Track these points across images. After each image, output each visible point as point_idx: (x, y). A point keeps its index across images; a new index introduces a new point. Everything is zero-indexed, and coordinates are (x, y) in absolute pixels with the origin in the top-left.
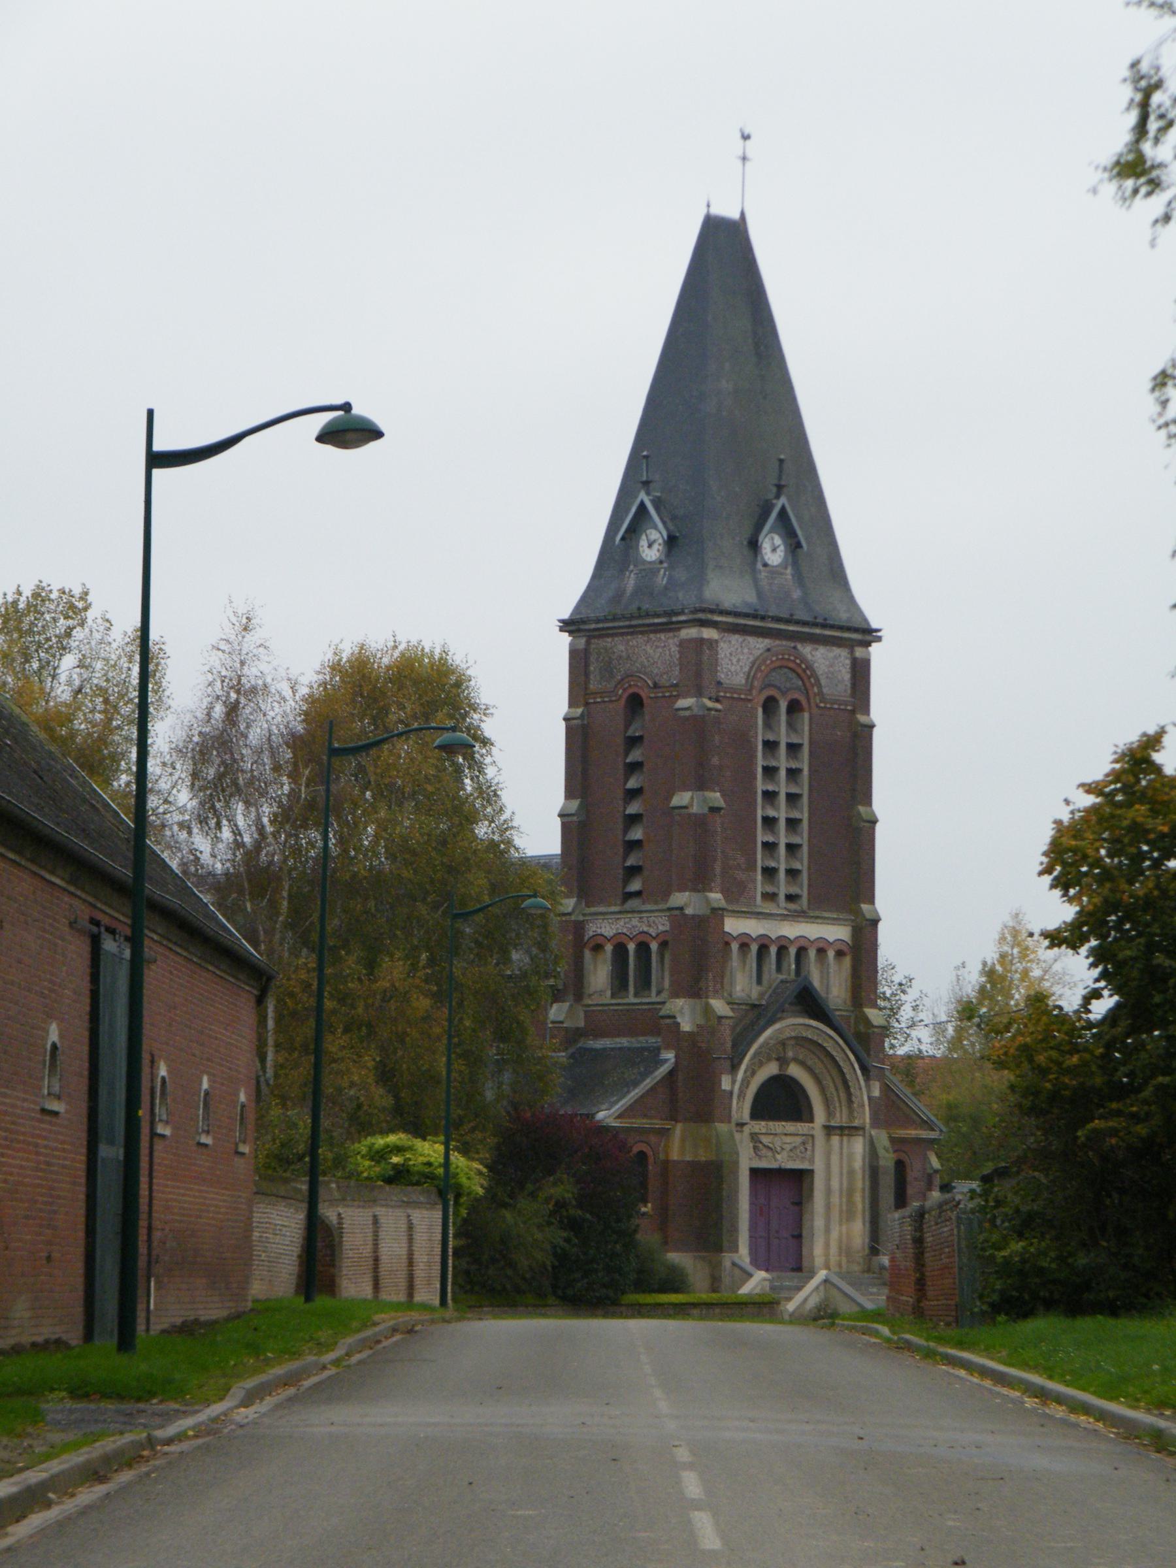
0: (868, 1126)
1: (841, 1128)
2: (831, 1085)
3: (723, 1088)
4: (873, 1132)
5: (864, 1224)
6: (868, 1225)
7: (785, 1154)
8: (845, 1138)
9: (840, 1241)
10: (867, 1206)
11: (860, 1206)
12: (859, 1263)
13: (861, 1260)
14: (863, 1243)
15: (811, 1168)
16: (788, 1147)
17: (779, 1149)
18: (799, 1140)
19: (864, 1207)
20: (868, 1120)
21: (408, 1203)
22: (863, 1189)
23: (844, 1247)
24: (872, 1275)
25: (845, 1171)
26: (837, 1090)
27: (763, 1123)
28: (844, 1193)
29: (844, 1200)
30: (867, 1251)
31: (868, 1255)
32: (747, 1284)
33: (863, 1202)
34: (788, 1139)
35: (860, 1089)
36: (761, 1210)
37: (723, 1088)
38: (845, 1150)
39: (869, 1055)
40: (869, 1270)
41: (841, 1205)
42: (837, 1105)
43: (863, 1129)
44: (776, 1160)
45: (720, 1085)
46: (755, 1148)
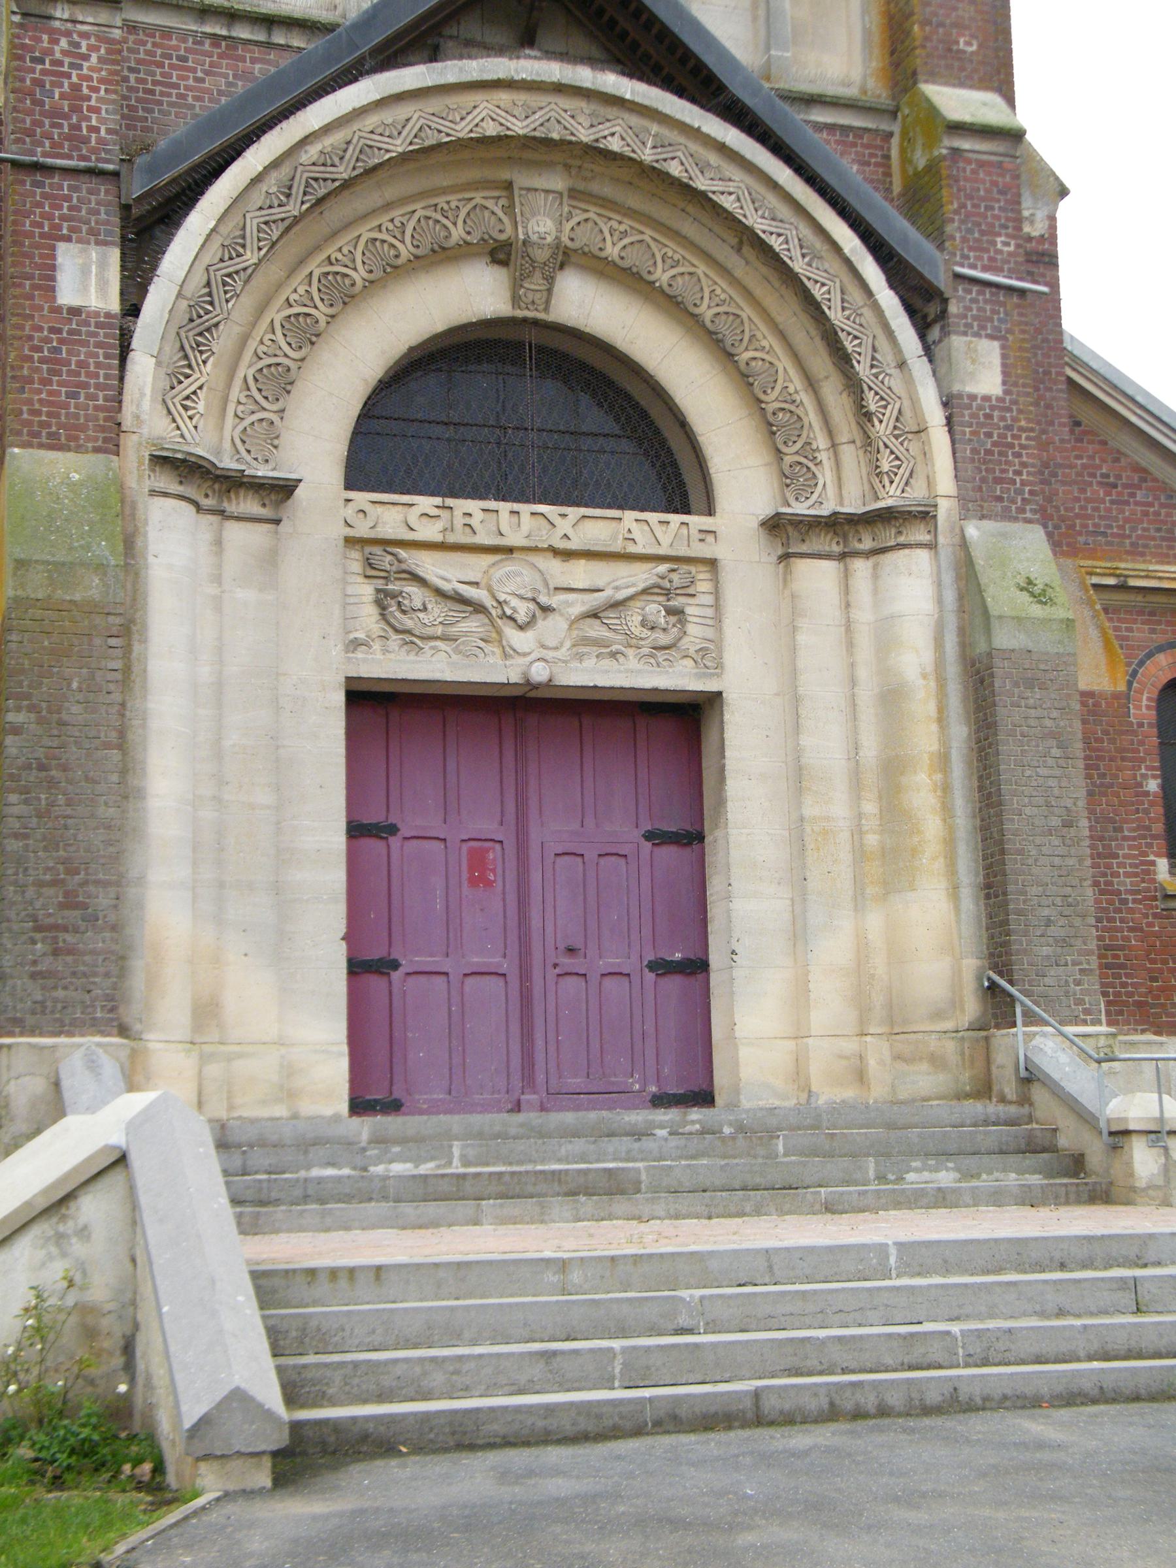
0: (946, 509)
1: (837, 524)
2: (784, 363)
3: (67, 295)
4: (973, 530)
5: (954, 892)
6: (968, 896)
7: (553, 628)
8: (860, 566)
9: (861, 967)
10: (963, 821)
11: (932, 827)
12: (936, 1061)
13: (950, 1047)
14: (957, 972)
15: (711, 686)
16: (579, 605)
17: (523, 610)
18: (641, 576)
19: (950, 829)
20: (945, 483)
21: (218, 754)
22: (943, 761)
23: (878, 999)
24: (993, 1108)
25: (866, 695)
26: (811, 384)
27: (426, 503)
28: (871, 778)
29: (870, 807)
30: (972, 1007)
31: (974, 1027)
32: (358, 1236)
33: (947, 809)
34: (580, 573)
35: (902, 365)
36: (478, 861)
37: (67, 295)
38: (864, 615)
39: (938, 237)
40: (984, 1089)
41: (858, 831)
42: (821, 442)
43: (925, 515)
44: (508, 652)
45: (50, 290)
46: (382, 600)
